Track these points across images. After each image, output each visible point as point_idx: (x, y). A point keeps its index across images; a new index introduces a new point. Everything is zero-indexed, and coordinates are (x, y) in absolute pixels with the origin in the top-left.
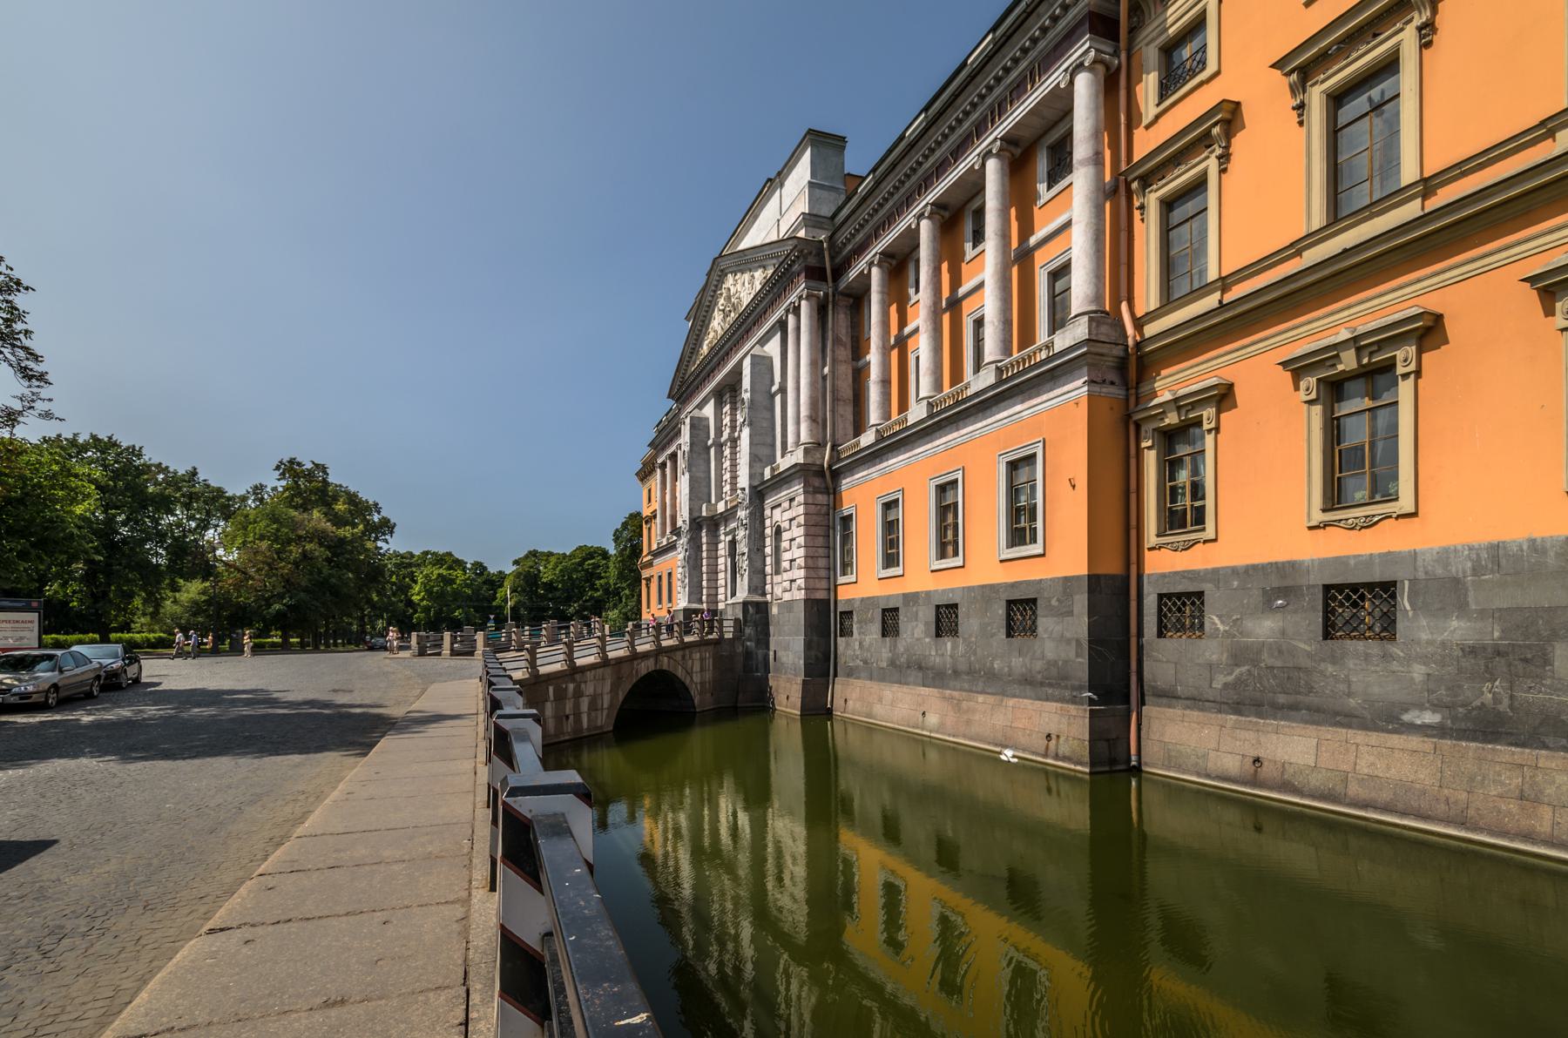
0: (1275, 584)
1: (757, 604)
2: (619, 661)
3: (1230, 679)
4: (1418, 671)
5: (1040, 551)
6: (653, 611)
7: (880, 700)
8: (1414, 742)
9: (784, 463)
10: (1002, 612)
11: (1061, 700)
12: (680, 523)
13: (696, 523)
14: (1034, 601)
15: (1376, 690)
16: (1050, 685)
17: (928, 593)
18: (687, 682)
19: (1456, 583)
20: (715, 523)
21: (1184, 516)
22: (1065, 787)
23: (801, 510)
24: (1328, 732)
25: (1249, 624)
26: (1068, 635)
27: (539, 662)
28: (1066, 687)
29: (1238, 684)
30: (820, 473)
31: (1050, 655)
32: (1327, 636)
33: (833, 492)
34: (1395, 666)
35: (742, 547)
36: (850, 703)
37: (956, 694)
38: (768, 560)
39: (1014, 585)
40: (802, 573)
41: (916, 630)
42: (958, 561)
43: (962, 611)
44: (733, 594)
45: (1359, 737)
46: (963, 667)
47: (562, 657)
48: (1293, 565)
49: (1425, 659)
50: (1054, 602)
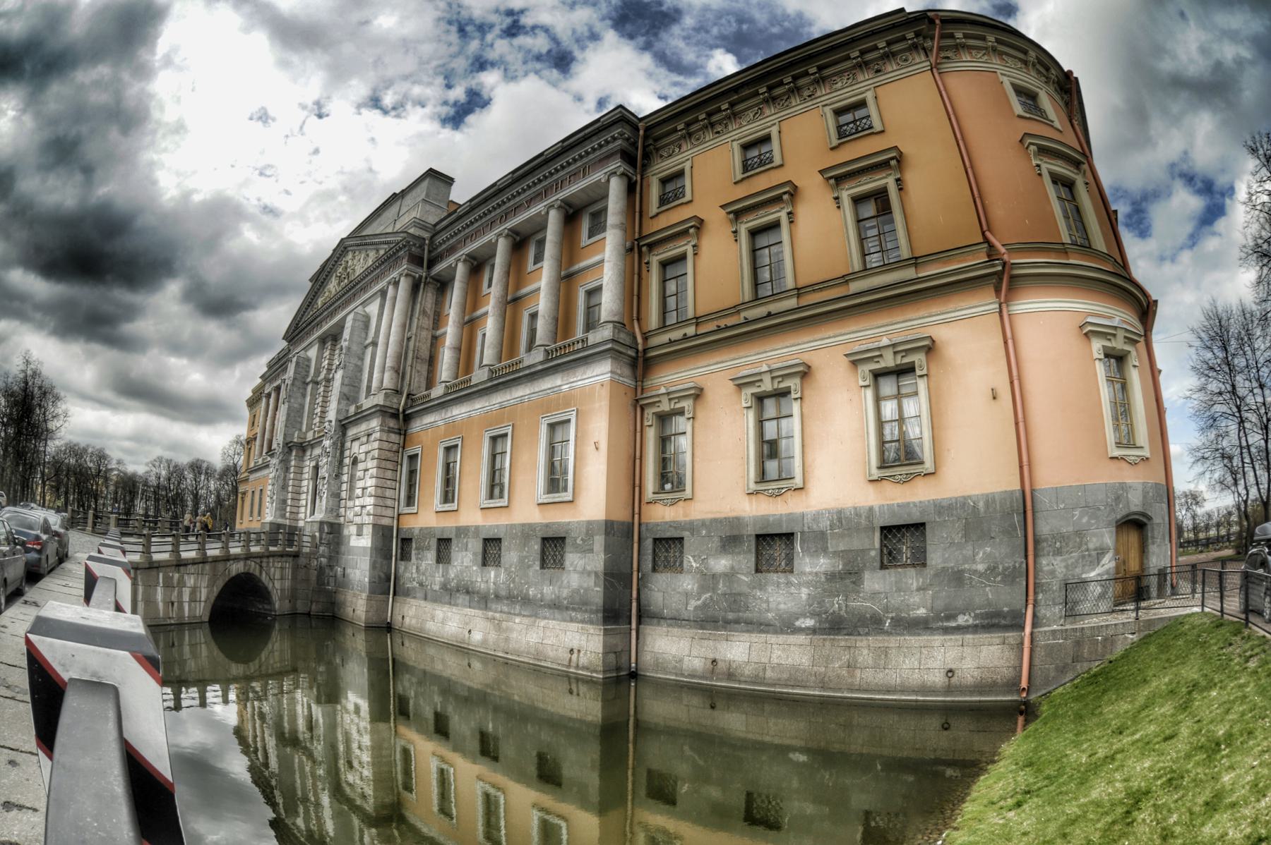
0: (730, 536)
1: (331, 525)
2: (216, 560)
3: (699, 602)
4: (804, 592)
5: (570, 498)
7: (433, 618)
8: (801, 639)
9: (366, 403)
10: (537, 547)
12: (274, 446)
13: (288, 447)
14: (563, 539)
15: (782, 606)
16: (574, 609)
17: (477, 528)
18: (270, 586)
23: (376, 445)
25: (712, 562)
26: (589, 568)
28: (586, 611)
29: (705, 605)
32: (757, 571)
33: (403, 432)
34: (793, 590)
35: (323, 472)
36: (407, 620)
37: (497, 615)
38: (344, 487)
39: (547, 525)
40: (370, 501)
41: (465, 560)
42: (504, 502)
43: (505, 544)
44: (313, 513)
45: (773, 639)
46: (503, 593)
47: (170, 548)
49: (808, 584)
50: (579, 541)
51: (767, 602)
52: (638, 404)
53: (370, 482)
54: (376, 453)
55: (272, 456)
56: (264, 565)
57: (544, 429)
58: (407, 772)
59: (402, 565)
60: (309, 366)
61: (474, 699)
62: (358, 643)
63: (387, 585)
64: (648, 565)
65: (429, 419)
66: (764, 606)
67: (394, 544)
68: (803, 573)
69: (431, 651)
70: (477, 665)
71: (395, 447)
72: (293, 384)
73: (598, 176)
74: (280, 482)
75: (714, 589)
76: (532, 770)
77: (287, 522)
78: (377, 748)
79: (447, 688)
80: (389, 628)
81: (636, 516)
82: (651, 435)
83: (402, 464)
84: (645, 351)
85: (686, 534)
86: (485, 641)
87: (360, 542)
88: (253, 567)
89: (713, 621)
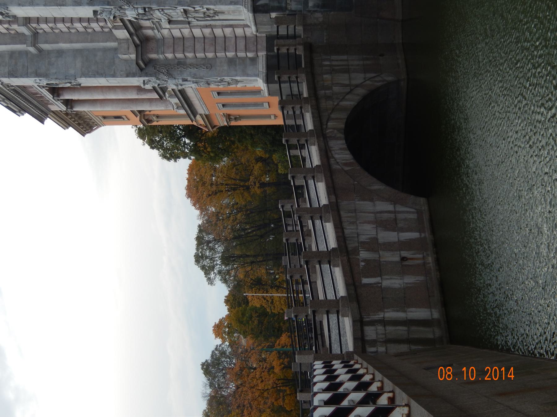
2: (331, 190)
6: (271, 114)
13: (145, 66)
18: (362, 91)
20: (142, 42)
27: (331, 296)
55: (164, 90)
72: (46, 76)
74: (202, 72)
77: (262, 54)
88: (336, 124)
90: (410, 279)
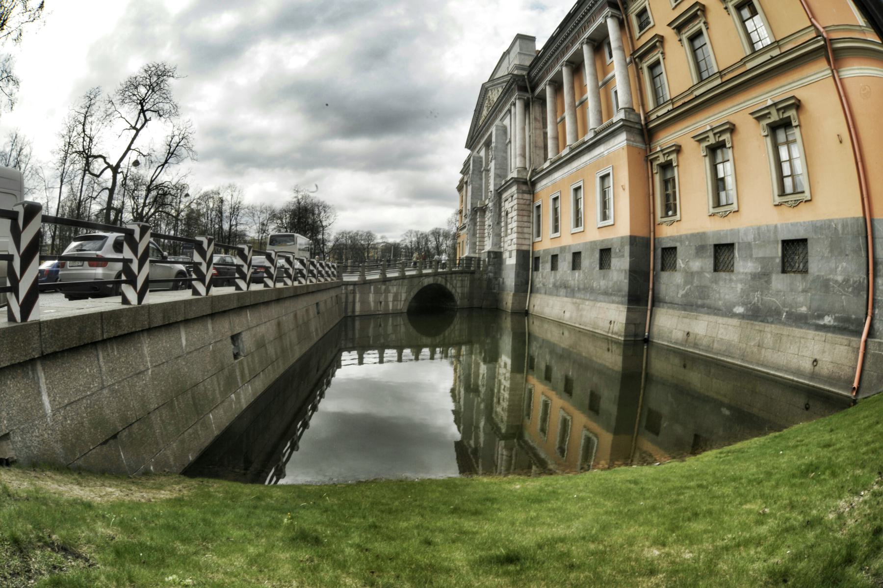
0: (699, 244)
1: (495, 253)
2: (412, 277)
4: (740, 286)
8: (735, 321)
10: (597, 255)
11: (618, 303)
14: (610, 249)
15: (727, 297)
16: (614, 295)
18: (453, 291)
19: (749, 244)
21: (670, 206)
22: (614, 347)
23: (515, 202)
24: (713, 318)
26: (622, 268)
30: (525, 183)
31: (615, 279)
32: (716, 270)
34: (733, 285)
36: (536, 307)
37: (578, 301)
38: (503, 229)
39: (602, 241)
40: (514, 236)
43: (583, 255)
46: (582, 286)
48: (704, 233)
49: (741, 281)
51: (719, 293)
52: (649, 160)
53: (514, 225)
54: (516, 207)
56: (449, 279)
57: (598, 180)
58: (529, 406)
59: (535, 273)
60: (481, 161)
61: (565, 355)
62: (507, 323)
63: (525, 286)
64: (659, 266)
65: (544, 182)
66: (717, 296)
67: (528, 261)
68: (739, 273)
69: (546, 326)
70: (566, 333)
71: (528, 202)
73: (600, 20)
74: (471, 232)
75: (692, 283)
76: (587, 402)
78: (512, 390)
79: (552, 348)
80: (526, 313)
81: (652, 234)
82: (657, 178)
83: (530, 212)
84: (647, 124)
85: (678, 245)
86: (571, 318)
87: (510, 261)
88: (440, 280)
89: (692, 305)
90: (372, 304)
